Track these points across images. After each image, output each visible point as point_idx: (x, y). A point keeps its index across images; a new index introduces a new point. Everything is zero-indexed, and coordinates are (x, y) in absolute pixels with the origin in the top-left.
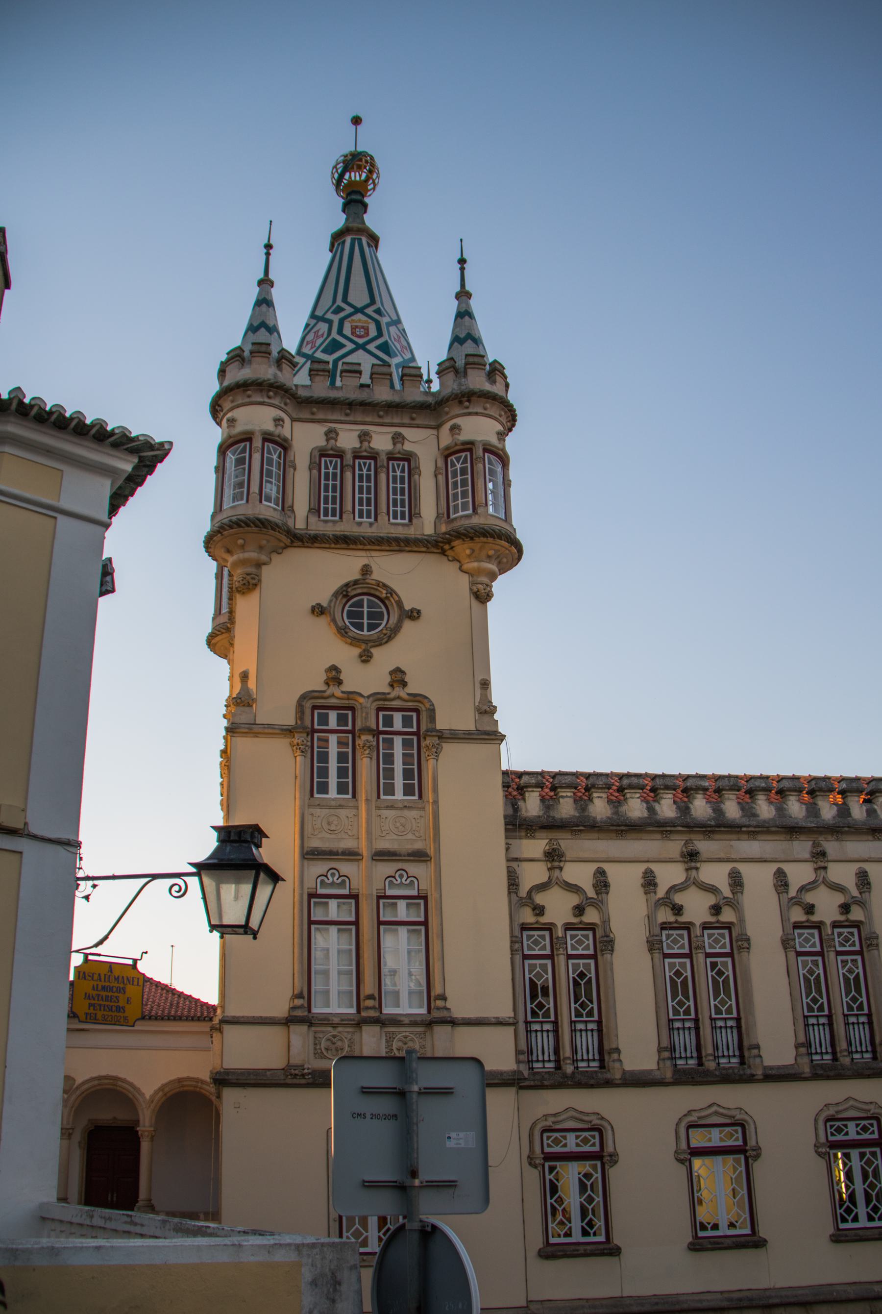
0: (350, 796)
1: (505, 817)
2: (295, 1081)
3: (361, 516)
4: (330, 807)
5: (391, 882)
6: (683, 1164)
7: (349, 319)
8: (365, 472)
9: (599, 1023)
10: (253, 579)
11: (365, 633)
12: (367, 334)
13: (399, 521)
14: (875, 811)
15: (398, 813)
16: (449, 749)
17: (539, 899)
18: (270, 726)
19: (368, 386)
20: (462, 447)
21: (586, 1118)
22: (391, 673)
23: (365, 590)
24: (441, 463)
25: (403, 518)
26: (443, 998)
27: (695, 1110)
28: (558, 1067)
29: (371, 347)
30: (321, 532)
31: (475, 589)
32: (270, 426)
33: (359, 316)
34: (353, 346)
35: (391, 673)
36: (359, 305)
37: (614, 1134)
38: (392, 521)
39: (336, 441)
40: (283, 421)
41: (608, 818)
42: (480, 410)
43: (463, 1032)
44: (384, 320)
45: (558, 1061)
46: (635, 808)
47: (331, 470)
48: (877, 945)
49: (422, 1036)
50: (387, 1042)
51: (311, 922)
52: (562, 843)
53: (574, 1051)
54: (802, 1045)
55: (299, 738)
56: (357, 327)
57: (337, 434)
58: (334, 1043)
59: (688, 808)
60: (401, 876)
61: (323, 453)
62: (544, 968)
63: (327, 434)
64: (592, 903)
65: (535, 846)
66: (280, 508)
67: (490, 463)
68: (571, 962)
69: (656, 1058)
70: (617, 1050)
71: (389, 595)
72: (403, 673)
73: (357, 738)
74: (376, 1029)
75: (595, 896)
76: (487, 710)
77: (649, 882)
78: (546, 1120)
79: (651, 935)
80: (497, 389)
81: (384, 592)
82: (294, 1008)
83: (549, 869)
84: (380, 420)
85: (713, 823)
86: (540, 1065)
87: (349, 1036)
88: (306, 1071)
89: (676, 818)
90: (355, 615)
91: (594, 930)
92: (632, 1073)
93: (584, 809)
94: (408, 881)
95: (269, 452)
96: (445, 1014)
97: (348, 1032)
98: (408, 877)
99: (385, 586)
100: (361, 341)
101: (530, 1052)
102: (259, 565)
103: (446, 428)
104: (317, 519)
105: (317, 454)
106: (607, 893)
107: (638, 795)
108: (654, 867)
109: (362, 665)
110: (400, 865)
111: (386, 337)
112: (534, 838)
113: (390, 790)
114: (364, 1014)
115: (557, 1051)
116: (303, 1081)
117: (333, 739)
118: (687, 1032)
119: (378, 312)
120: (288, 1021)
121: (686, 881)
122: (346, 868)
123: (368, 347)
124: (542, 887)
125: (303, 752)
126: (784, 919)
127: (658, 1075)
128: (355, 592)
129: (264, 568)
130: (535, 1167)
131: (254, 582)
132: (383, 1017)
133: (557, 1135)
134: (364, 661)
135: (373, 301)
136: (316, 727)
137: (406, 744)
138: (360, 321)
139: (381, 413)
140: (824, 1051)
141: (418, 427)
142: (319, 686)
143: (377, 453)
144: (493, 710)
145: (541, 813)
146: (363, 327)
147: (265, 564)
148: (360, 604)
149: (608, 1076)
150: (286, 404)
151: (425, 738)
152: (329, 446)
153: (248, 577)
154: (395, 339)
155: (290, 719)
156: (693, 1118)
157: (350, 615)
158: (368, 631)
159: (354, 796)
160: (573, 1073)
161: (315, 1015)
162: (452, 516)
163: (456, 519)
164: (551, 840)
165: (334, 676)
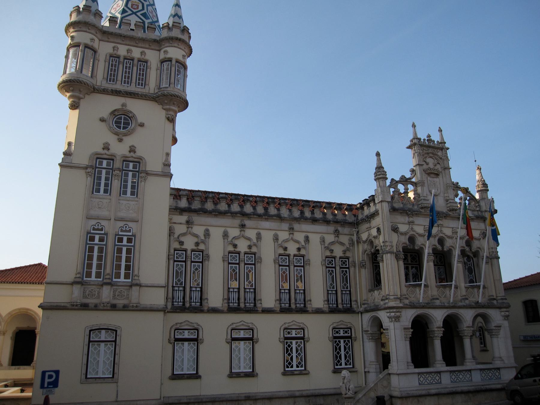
0: (109, 194)
1: (170, 206)
2: (73, 307)
3: (125, 83)
4: (100, 198)
5: (121, 229)
6: (228, 344)
8: (128, 65)
10: (77, 104)
11: (122, 130)
12: (138, 8)
13: (140, 87)
16: (150, 179)
17: (182, 239)
19: (133, 30)
20: (168, 59)
21: (193, 325)
23: (123, 113)
24: (159, 65)
25: (142, 85)
27: (235, 323)
28: (184, 305)
29: (139, 14)
30: (107, 88)
31: (167, 116)
32: (88, 42)
34: (131, 12)
35: (130, 147)
37: (203, 331)
39: (117, 51)
40: (94, 40)
42: (176, 45)
44: (146, 4)
45: (184, 302)
46: (223, 206)
47: (114, 63)
48: (309, 264)
49: (128, 290)
50: (113, 292)
51: (87, 244)
52: (193, 218)
53: (191, 298)
54: (278, 300)
56: (134, 4)
57: (118, 49)
58: (92, 292)
60: (126, 227)
61: (111, 56)
62: (182, 266)
63: (114, 48)
64: (203, 242)
65: (183, 218)
68: (192, 264)
70: (207, 299)
71: (132, 116)
72: (136, 148)
73: (114, 172)
74: (109, 287)
76: (168, 165)
77: (225, 235)
78: (177, 325)
79: (224, 255)
80: (185, 37)
81: (131, 114)
82: (75, 278)
83: (188, 228)
84: (136, 45)
85: (252, 214)
86: (176, 303)
87: (98, 290)
88: (78, 303)
89: (239, 211)
90: (118, 123)
91: (202, 252)
94: (128, 229)
96: (138, 282)
97: (98, 288)
98: (129, 227)
99: (131, 112)
100: (135, 11)
101: (173, 298)
102: (80, 99)
103: (162, 51)
104: (106, 82)
107: (225, 201)
109: (119, 143)
111: (145, 11)
113: (125, 193)
114: (105, 281)
115: (184, 298)
116: (76, 308)
117: (104, 171)
118: (235, 293)
120: (73, 283)
121: (240, 235)
122: (103, 223)
123: (137, 14)
124: (184, 234)
125: (90, 175)
128: (118, 114)
129: (81, 100)
130: (171, 343)
131: (76, 105)
133: (181, 331)
134: (119, 141)
136: (97, 166)
139: (137, 42)
140: (286, 302)
141: (152, 49)
142: (99, 150)
143: (134, 58)
144: (169, 165)
146: (136, 5)
147: (82, 99)
148: (121, 118)
149: (202, 309)
151: (141, 174)
152: (114, 53)
153: (74, 103)
156: (234, 326)
157: (116, 122)
158: (123, 129)
159: (110, 195)
160: (189, 307)
161: (85, 281)
162: (161, 87)
163: (162, 88)
164: (189, 216)
165: (106, 147)
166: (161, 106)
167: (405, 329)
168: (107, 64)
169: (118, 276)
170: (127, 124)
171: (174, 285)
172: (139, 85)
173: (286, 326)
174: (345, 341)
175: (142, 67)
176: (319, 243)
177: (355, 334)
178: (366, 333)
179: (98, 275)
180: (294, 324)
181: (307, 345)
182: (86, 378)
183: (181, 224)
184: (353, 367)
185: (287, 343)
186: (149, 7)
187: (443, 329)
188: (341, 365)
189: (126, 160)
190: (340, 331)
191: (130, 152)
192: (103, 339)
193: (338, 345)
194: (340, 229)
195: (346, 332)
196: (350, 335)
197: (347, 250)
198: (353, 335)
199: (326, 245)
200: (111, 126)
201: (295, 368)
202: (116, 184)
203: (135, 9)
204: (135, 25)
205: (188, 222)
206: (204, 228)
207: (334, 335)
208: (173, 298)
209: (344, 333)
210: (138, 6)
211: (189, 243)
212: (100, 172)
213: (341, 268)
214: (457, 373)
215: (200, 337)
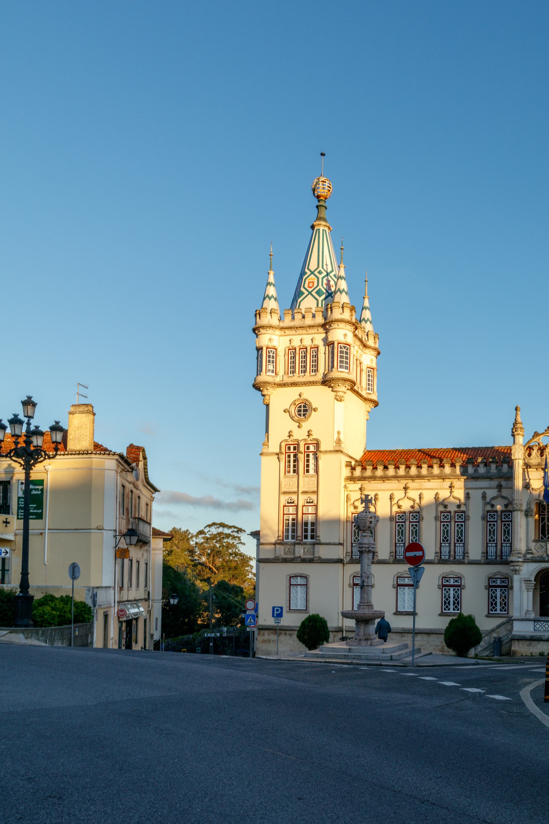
7: (308, 278)
11: (302, 417)
12: (313, 285)
14: (478, 470)
18: (272, 453)
33: (312, 276)
36: (313, 270)
38: (312, 374)
41: (381, 476)
44: (321, 277)
56: (310, 282)
59: (409, 471)
65: (358, 485)
66: (274, 374)
69: (389, 555)
74: (300, 546)
89: (404, 475)
92: (380, 560)
93: (374, 473)
96: (318, 541)
100: (310, 290)
101: (352, 552)
105: (287, 349)
110: (309, 496)
111: (320, 287)
112: (357, 483)
119: (320, 273)
126: (437, 510)
127: (388, 561)
135: (318, 267)
138: (312, 278)
139: (308, 330)
145: (360, 475)
146: (312, 282)
156: (399, 575)
166: (331, 389)
168: (287, 357)
169: (306, 537)
170: (305, 411)
171: (353, 542)
172: (312, 372)
173: (444, 575)
174: (501, 590)
176: (481, 499)
178: (526, 582)
179: (293, 537)
181: (463, 591)
182: (290, 609)
183: (356, 491)
184: (508, 613)
185: (445, 589)
188: (496, 610)
190: (497, 581)
192: (299, 583)
193: (494, 593)
194: (503, 483)
195: (503, 582)
196: (507, 584)
197: (510, 504)
198: (510, 585)
199: (488, 500)
200: (294, 415)
203: (310, 287)
205: (361, 489)
207: (490, 584)
208: (352, 552)
209: (501, 583)
210: (313, 283)
212: (289, 456)
213: (502, 521)
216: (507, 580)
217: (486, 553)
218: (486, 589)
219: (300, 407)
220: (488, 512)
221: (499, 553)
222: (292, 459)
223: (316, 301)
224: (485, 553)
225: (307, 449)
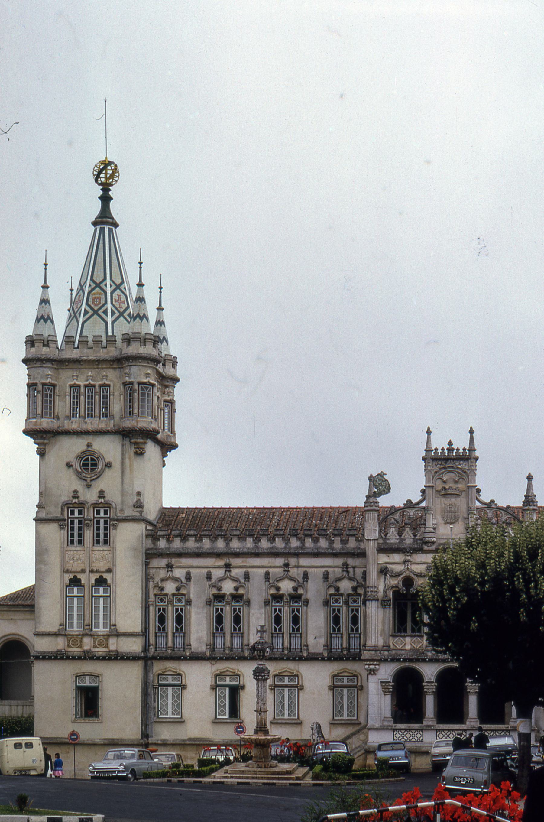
3: (88, 417)
8: (90, 394)
9: (184, 633)
12: (100, 303)
15: (101, 552)
22: (99, 492)
26: (115, 625)
33: (98, 289)
36: (98, 281)
43: (122, 640)
55: (61, 523)
56: (95, 298)
67: (142, 389)
75: (185, 582)
90: (85, 465)
95: (46, 391)
96: (115, 633)
100: (96, 308)
102: (45, 444)
106: (190, 581)
108: (211, 570)
124: (162, 580)
132: (92, 633)
137: (106, 522)
138: (97, 293)
148: (87, 459)
150: (53, 364)
154: (115, 300)
155: (58, 515)
167: (381, 682)
170: (95, 465)
175: (105, 394)
177: (361, 682)
180: (286, 671)
186: (114, 295)
187: (436, 684)
189: (96, 506)
191: (100, 497)
195: (351, 680)
196: (356, 684)
198: (359, 684)
201: (286, 716)
202: (88, 535)
203: (96, 305)
204: (93, 341)
206: (184, 571)
211: (170, 588)
214: (446, 732)
215: (184, 683)
216: (356, 678)
217: (328, 646)
218: (331, 689)
219: (87, 459)
220: (331, 595)
221: (345, 645)
222: (76, 525)
223: (104, 324)
224: (327, 646)
225: (97, 515)
